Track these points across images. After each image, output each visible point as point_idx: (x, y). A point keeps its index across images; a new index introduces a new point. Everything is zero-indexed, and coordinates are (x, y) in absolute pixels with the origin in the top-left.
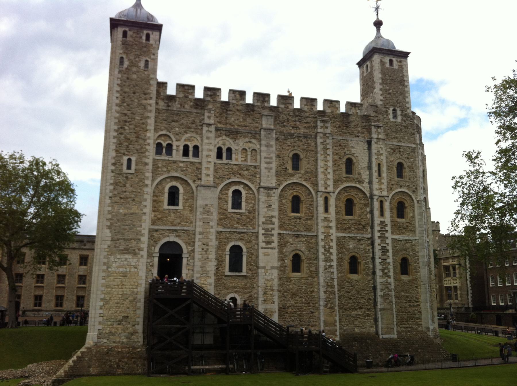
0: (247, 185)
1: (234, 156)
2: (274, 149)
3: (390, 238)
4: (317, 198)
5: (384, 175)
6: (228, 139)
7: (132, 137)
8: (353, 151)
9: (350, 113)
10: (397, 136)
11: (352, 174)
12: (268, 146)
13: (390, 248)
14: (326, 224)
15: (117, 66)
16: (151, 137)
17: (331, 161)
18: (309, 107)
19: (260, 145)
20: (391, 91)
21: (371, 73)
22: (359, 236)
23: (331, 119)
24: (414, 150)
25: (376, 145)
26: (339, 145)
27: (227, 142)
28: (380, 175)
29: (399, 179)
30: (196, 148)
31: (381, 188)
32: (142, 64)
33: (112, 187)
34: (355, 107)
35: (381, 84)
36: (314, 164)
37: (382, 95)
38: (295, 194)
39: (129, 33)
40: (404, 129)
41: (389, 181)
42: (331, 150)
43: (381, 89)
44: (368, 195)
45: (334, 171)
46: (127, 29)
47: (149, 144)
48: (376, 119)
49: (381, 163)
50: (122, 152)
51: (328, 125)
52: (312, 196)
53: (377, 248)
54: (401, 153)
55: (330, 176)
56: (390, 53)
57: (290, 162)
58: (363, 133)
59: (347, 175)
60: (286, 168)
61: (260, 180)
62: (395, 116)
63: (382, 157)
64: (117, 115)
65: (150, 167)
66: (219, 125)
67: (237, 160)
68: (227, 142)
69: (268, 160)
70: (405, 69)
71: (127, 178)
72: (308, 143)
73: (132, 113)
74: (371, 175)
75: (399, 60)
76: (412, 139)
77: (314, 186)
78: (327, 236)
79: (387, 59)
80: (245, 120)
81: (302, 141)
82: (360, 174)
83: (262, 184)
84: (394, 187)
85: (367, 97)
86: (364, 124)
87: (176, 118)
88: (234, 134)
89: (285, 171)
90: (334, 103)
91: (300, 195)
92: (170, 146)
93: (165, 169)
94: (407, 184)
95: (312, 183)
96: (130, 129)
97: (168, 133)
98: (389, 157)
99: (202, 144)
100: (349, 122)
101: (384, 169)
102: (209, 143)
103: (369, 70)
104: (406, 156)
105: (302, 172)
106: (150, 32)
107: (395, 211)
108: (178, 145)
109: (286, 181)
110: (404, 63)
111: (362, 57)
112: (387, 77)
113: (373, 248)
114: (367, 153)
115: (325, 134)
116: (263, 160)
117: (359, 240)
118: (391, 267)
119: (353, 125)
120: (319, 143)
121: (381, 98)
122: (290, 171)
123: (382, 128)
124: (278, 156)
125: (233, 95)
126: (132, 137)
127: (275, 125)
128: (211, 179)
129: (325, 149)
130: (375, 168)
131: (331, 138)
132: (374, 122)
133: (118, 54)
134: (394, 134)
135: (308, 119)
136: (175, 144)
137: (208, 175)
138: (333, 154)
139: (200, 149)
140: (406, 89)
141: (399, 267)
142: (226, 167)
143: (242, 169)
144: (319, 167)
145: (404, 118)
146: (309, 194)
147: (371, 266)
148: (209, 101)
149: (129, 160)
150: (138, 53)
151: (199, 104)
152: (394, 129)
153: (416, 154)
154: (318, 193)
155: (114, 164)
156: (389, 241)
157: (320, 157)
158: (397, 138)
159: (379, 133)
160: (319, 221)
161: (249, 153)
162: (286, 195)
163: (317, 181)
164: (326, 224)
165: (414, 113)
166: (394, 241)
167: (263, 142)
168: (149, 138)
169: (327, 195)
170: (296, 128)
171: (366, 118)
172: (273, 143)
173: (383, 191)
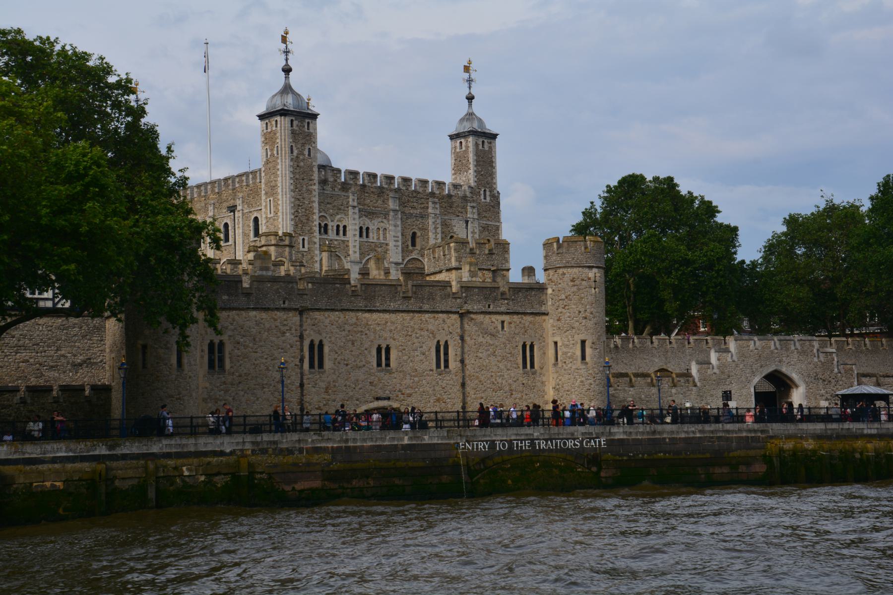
1: (371, 234)
2: (399, 228)
7: (304, 219)
8: (455, 229)
12: (396, 226)
21: (466, 151)
26: (445, 224)
27: (367, 223)
32: (306, 152)
39: (295, 123)
62: (485, 198)
65: (317, 246)
92: (326, 225)
100: (452, 203)
108: (332, 225)
115: (436, 215)
122: (410, 248)
124: (402, 235)
128: (358, 255)
136: (330, 224)
149: (303, 240)
150: (303, 141)
151: (345, 187)
171: (464, 198)
172: (399, 223)
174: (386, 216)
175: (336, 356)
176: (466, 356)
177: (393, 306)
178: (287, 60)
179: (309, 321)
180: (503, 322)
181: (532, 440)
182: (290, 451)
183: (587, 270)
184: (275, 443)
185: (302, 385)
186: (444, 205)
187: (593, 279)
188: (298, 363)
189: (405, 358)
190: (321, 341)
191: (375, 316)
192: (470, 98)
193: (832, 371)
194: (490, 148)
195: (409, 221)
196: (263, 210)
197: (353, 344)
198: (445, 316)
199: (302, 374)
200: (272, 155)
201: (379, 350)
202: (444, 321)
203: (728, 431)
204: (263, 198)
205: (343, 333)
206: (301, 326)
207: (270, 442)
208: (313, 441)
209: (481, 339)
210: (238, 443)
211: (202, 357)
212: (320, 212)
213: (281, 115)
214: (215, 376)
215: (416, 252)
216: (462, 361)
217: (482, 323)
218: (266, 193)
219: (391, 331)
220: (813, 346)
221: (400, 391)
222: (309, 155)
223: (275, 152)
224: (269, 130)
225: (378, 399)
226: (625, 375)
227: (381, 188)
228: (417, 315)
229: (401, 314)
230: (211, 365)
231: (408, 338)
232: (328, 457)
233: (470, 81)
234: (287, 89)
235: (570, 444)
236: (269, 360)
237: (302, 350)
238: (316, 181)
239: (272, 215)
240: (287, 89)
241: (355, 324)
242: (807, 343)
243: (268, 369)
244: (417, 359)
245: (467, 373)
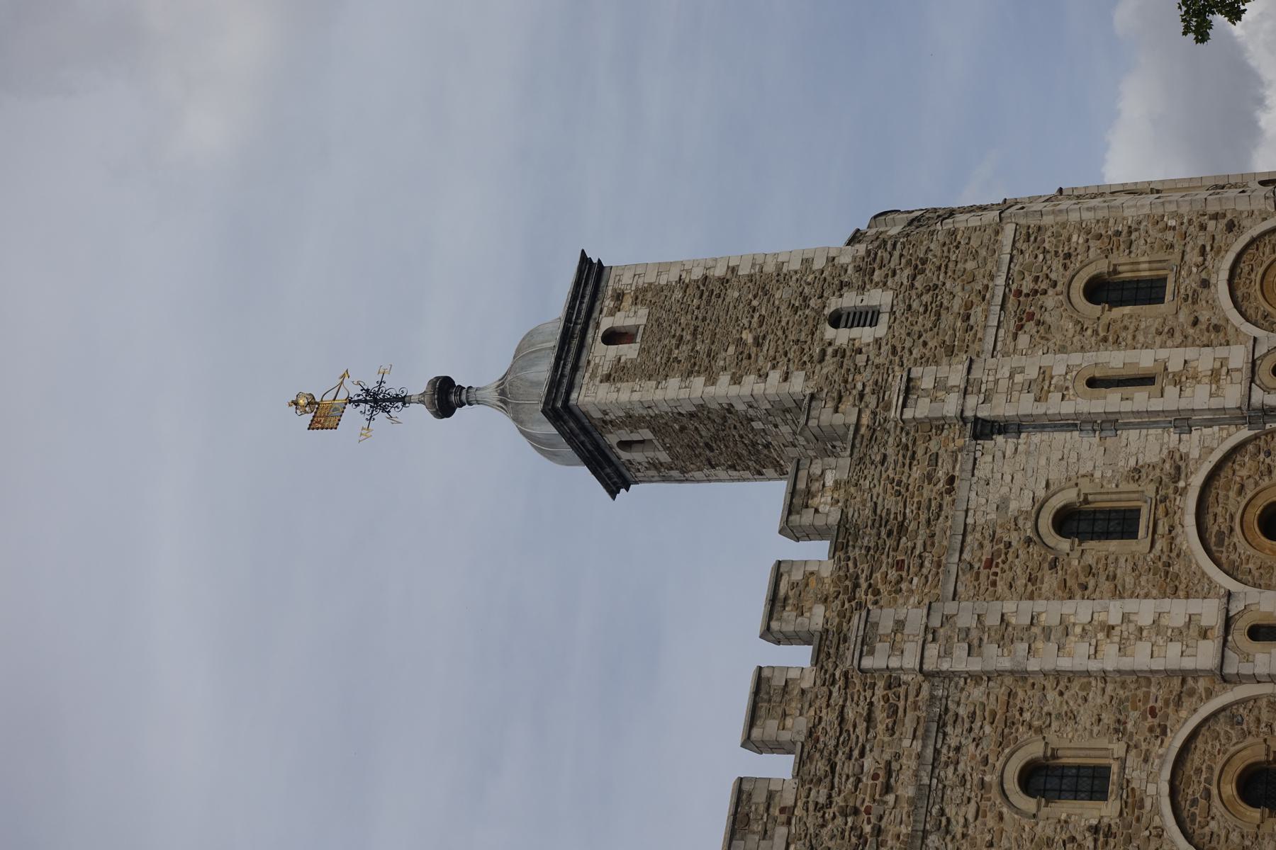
4: (1255, 679)
5: (1145, 360)
9: (834, 517)
10: (957, 305)
11: (1137, 511)
17: (1068, 607)
20: (748, 337)
23: (860, 606)
24: (1030, 235)
25: (999, 399)
26: (991, 568)
28: (1145, 380)
29: (1168, 297)
34: (809, 493)
35: (711, 380)
36: (1076, 686)
37: (763, 376)
38: (1230, 789)
41: (1178, 338)
42: (1009, 607)
43: (736, 380)
44: (1245, 433)
45: (1118, 594)
48: (871, 400)
49: (1088, 375)
51: (885, 619)
52: (1243, 702)
54: (1043, 285)
55: (1144, 611)
56: (575, 342)
57: (1064, 809)
59: (1141, 533)
60: (1095, 830)
62: (867, 317)
63: (1059, 370)
70: (651, 278)
72: (973, 716)
74: (1146, 420)
75: (609, 303)
76: (975, 243)
77: (1192, 693)
79: (602, 355)
81: (958, 749)
84: (1204, 316)
85: (768, 446)
86: (890, 451)
89: (1109, 834)
90: (782, 591)
91: (1238, 766)
94: (1193, 257)
95: (1179, 703)
98: (1057, 338)
100: (879, 521)
101: (1115, 360)
103: (646, 434)
104: (1057, 264)
105: (1118, 748)
109: (1160, 832)
110: (627, 279)
111: (584, 471)
112: (682, 353)
115: (931, 633)
120: (975, 665)
121: (775, 376)
122: (1108, 810)
123: (916, 372)
129: (1005, 633)
130: (1112, 401)
131: (950, 607)
132: (887, 408)
134: (947, 320)
135: (850, 714)
138: (1031, 597)
140: (744, 271)
144: (1094, 666)
145: (877, 276)
146: (1235, 721)
152: (924, 322)
153: (1048, 220)
154: (1230, 669)
157: (1046, 658)
158: (969, 306)
159: (940, 385)
162: (1235, 837)
163: (1169, 674)
165: (855, 238)
169: (1242, 625)
170: (889, 773)
173: (1224, 361)
194: (639, 297)
215: (1136, 774)
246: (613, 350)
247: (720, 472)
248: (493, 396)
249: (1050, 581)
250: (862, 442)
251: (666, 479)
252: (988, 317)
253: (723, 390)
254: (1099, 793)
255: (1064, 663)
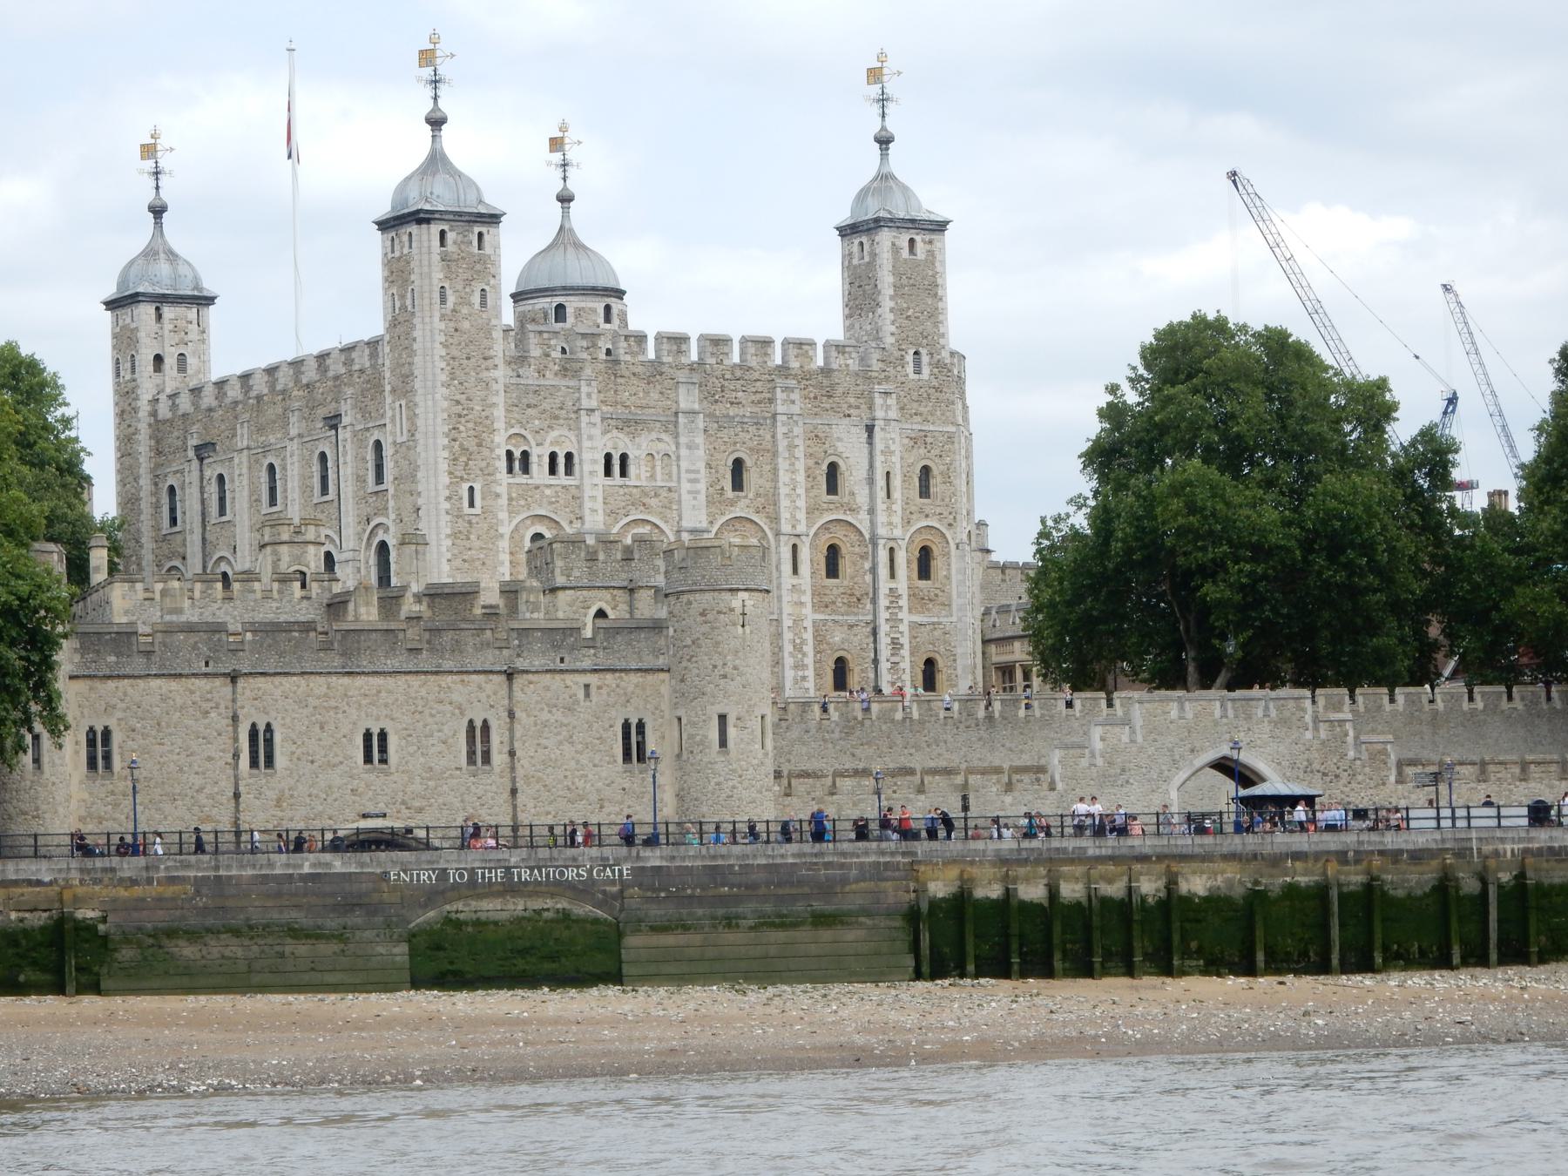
0: (657, 527)
1: (632, 469)
2: (701, 452)
3: (906, 622)
6: (621, 435)
7: (471, 444)
8: (840, 447)
9: (834, 366)
13: (905, 640)
14: (795, 597)
15: (437, 306)
16: (500, 443)
17: (802, 472)
18: (760, 359)
19: (678, 445)
21: (871, 265)
22: (852, 619)
24: (951, 438)
26: (816, 437)
30: (569, 456)
31: (895, 523)
32: (476, 299)
33: (449, 542)
35: (892, 298)
39: (450, 236)
40: (935, 395)
43: (892, 310)
44: (867, 537)
46: (446, 228)
47: (499, 458)
50: (458, 474)
51: (795, 396)
53: (884, 641)
55: (802, 503)
57: (729, 476)
58: (858, 407)
61: (680, 516)
62: (918, 371)
64: (445, 404)
65: (504, 501)
66: (604, 408)
67: (638, 477)
68: (619, 443)
69: (693, 476)
70: (939, 257)
71: (470, 522)
73: (469, 399)
75: (927, 238)
78: (797, 621)
79: (904, 239)
80: (647, 393)
82: (852, 494)
83: (685, 524)
84: (914, 517)
87: (532, 399)
88: (630, 425)
92: (525, 455)
93: (522, 502)
94: (938, 510)
96: (467, 430)
97: (523, 432)
99: (580, 449)
101: (897, 482)
102: (592, 448)
103: (867, 259)
104: (937, 452)
105: (751, 495)
106: (484, 229)
107: (915, 566)
112: (904, 281)
113: (875, 641)
114: (865, 449)
115: (790, 416)
116: (683, 475)
117: (851, 627)
118: (907, 677)
119: (840, 390)
120: (779, 436)
121: (893, 328)
122: (729, 493)
124: (709, 466)
125: (625, 344)
126: (471, 444)
127: (701, 401)
129: (791, 447)
130: (880, 482)
133: (435, 282)
134: (915, 405)
136: (535, 452)
137: (594, 511)
139: (576, 460)
140: (940, 305)
141: (920, 677)
142: (622, 491)
143: (646, 495)
147: (872, 676)
148: (583, 361)
149: (471, 489)
150: (468, 275)
155: (448, 498)
156: (904, 627)
157: (783, 464)
159: (888, 407)
160: (784, 592)
161: (658, 463)
164: (795, 597)
166: (914, 626)
167: (683, 440)
168: (498, 446)
172: (700, 439)
174: (671, 424)
175: (294, 748)
176: (516, 745)
177: (391, 664)
178: (436, 98)
179: (248, 692)
180: (587, 686)
181: (508, 869)
182: (134, 882)
183: (727, 596)
184: (113, 870)
185: (237, 796)
186: (813, 392)
187: (739, 610)
188: (230, 760)
189: (412, 749)
190: (268, 725)
191: (360, 681)
192: (884, 141)
193: (1343, 756)
194: (931, 253)
195: (724, 434)
196: (389, 427)
197: (322, 728)
198: (482, 677)
199: (236, 778)
200: (404, 308)
201: (368, 736)
202: (480, 687)
203: (844, 854)
204: (389, 400)
205: (305, 711)
206: (234, 701)
207: (105, 870)
208: (167, 868)
209: (545, 716)
210: (60, 871)
211: (77, 752)
212: (509, 425)
213: (420, 222)
214: (98, 783)
215: (743, 503)
216: (512, 753)
217: (547, 688)
218: (393, 391)
219: (386, 705)
220: (1304, 710)
221: (403, 802)
222: (483, 303)
223: (409, 302)
224: (397, 254)
225: (365, 816)
226: (998, 771)
227: (657, 363)
228: (432, 678)
229: (404, 678)
230: (92, 763)
231: (417, 716)
232: (190, 889)
233: (883, 100)
234: (436, 162)
235: (570, 874)
236: (183, 756)
237: (236, 740)
238: (499, 361)
239: (404, 438)
240: (436, 162)
241: (326, 695)
242: (1291, 704)
243: (181, 770)
244: (433, 750)
245: (520, 772)
246: (906, 244)
247: (847, 286)
248: (884, 171)
249: (811, 462)
250: (865, 375)
251: (843, 257)
252: (916, 425)
253: (887, 304)
254: (734, 489)
255: (781, 473)
